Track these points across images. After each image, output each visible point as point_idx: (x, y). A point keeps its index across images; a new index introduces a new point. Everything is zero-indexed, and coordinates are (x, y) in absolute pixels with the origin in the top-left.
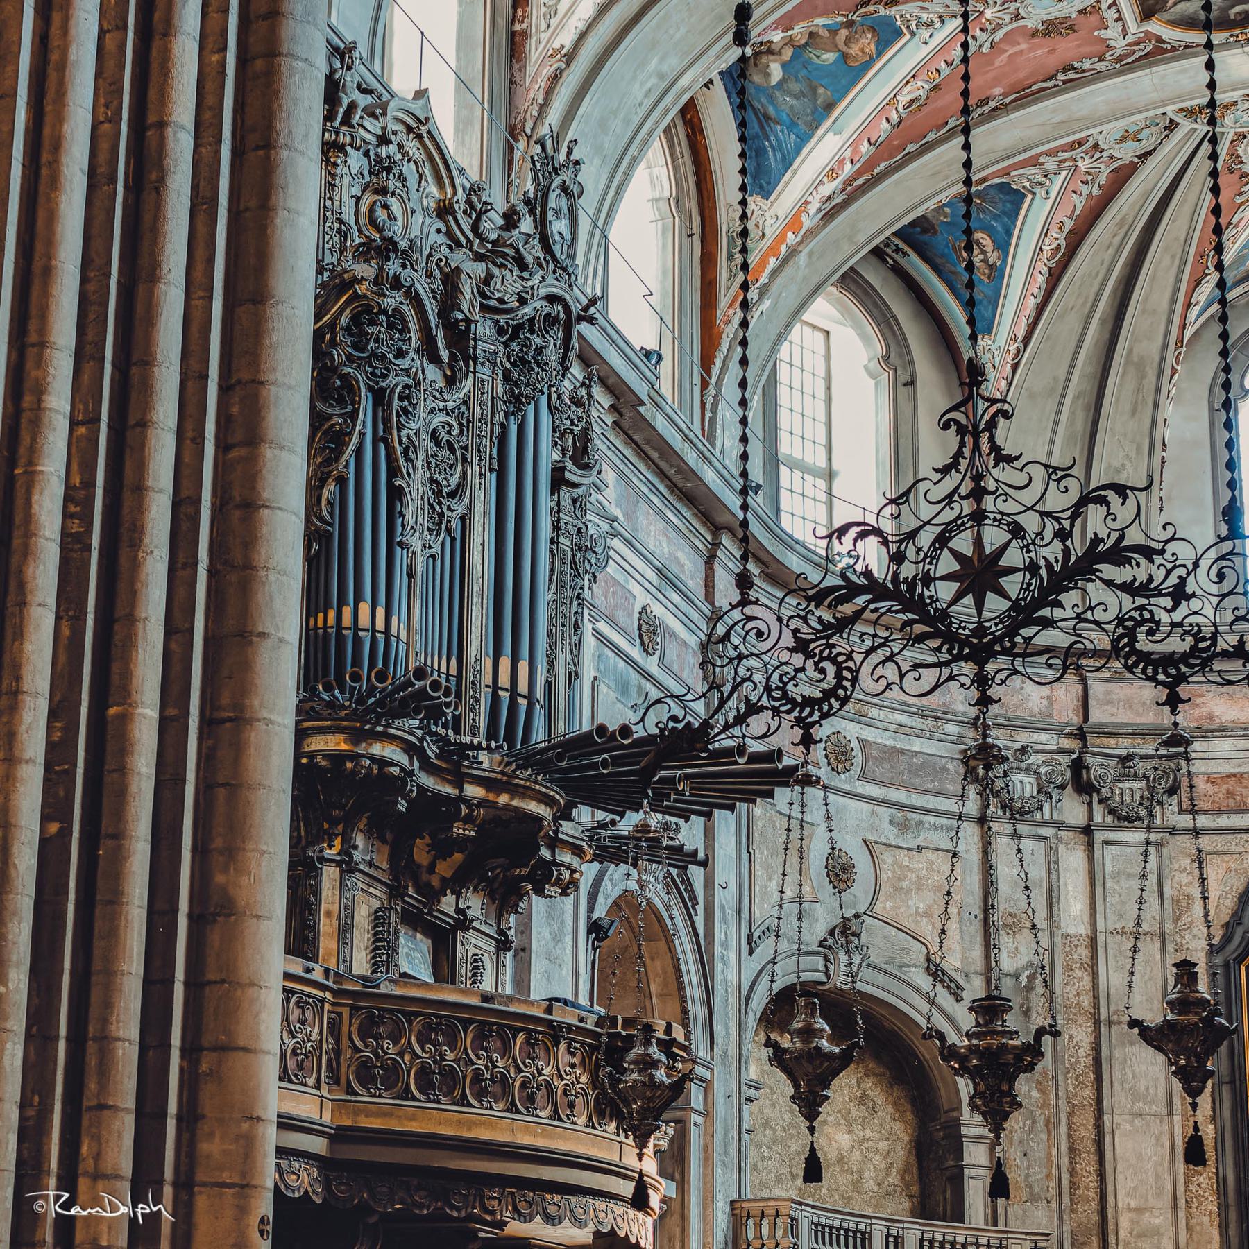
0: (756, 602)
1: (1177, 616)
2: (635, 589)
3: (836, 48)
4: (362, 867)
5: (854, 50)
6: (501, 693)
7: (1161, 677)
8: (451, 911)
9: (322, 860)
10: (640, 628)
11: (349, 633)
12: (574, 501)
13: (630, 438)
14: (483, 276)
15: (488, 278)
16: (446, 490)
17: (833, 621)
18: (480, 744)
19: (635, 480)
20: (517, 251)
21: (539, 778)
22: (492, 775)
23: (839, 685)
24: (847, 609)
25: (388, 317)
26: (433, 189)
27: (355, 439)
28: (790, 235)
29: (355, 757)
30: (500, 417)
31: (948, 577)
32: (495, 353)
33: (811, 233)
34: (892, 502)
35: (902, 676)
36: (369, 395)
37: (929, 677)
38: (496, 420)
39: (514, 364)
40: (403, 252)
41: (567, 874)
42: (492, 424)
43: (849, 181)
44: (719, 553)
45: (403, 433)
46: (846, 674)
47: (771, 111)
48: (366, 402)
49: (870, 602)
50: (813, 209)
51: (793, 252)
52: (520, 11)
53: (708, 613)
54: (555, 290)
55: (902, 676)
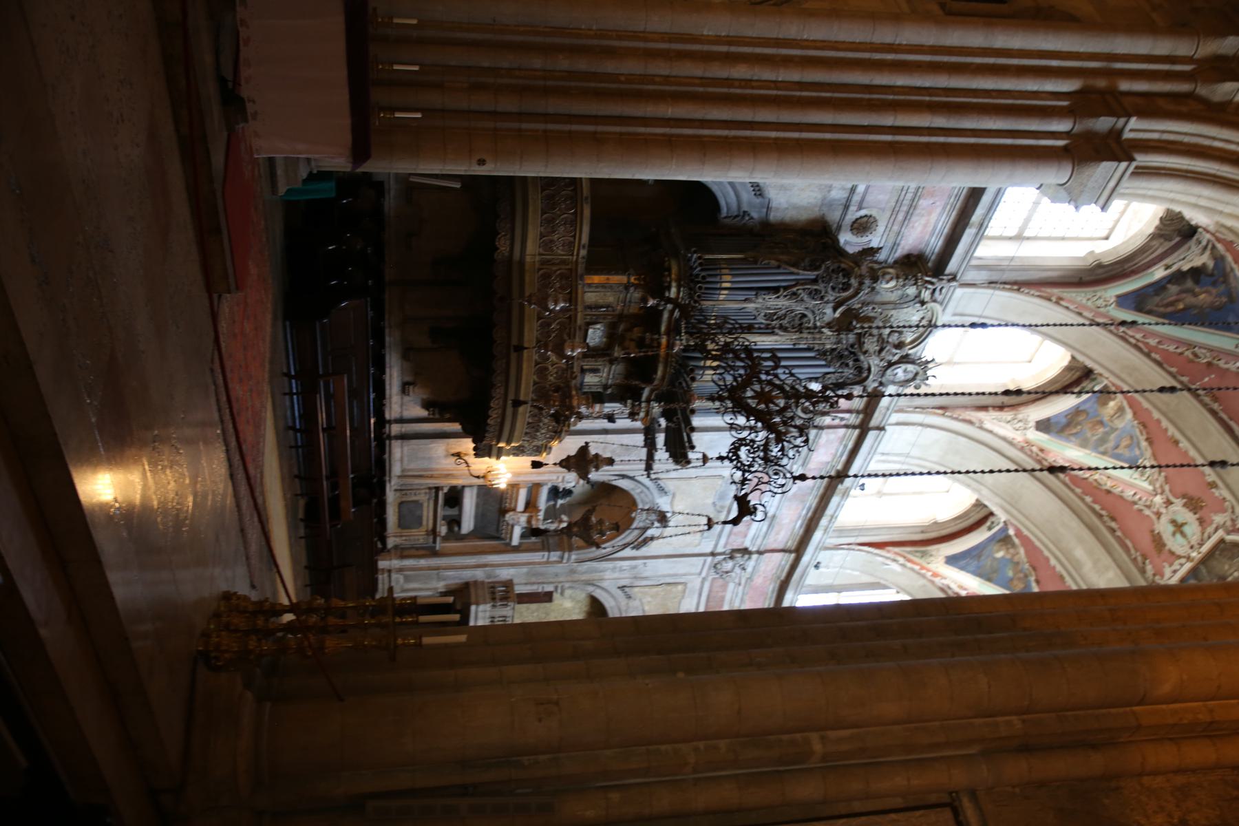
1: (757, 459)
3: (1015, 574)
5: (1015, 582)
7: (731, 455)
9: (629, 274)
11: (718, 272)
26: (909, 340)
27: (793, 270)
28: (930, 574)
29: (670, 275)
30: (817, 347)
31: (762, 388)
32: (842, 344)
33: (932, 582)
36: (814, 277)
37: (721, 383)
39: (839, 353)
47: (983, 558)
48: (812, 275)
50: (945, 582)
51: (924, 576)
52: (997, 409)
54: (873, 369)
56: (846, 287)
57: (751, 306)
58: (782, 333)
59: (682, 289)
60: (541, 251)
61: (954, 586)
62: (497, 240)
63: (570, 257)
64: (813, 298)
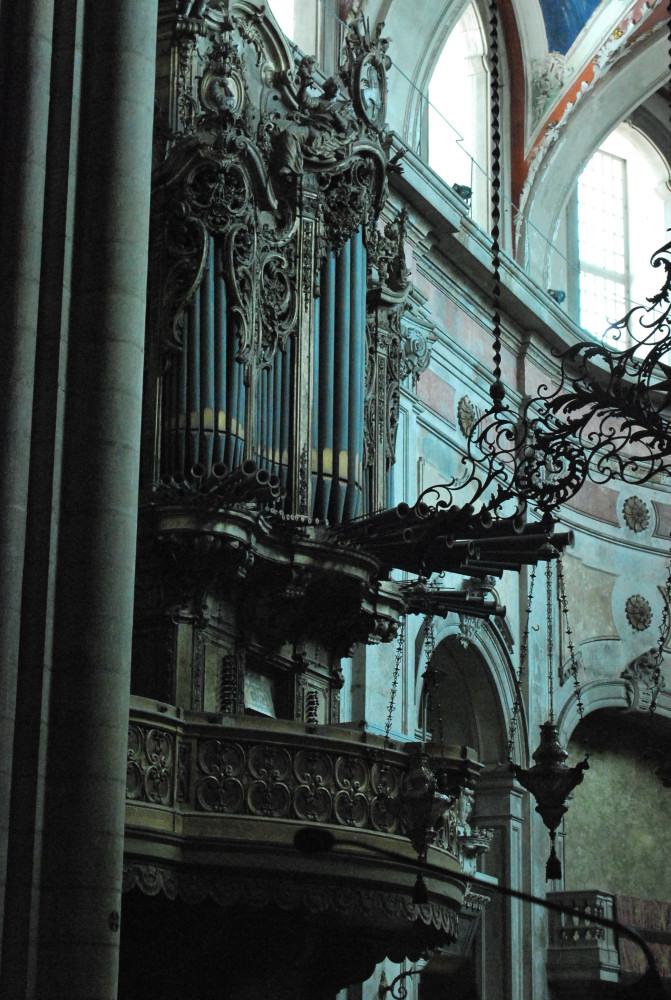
0: (506, 409)
2: (455, 383)
4: (211, 623)
6: (325, 478)
8: (289, 657)
10: (459, 416)
11: (196, 434)
12: (390, 317)
13: (447, 257)
14: (306, 137)
15: (310, 140)
16: (277, 314)
17: (567, 424)
18: (306, 521)
19: (453, 293)
20: (334, 116)
21: (358, 547)
22: (318, 546)
23: (572, 475)
24: (577, 415)
25: (226, 175)
26: (271, 65)
27: (200, 275)
28: (584, 84)
30: (322, 252)
32: (317, 200)
33: (600, 81)
34: (615, 326)
35: (622, 467)
36: (212, 239)
38: (319, 255)
39: (333, 209)
40: (238, 121)
41: (386, 625)
42: (315, 258)
43: (632, 39)
44: (528, 351)
45: (240, 269)
46: (578, 466)
48: (208, 245)
49: (594, 409)
50: (603, 61)
51: (587, 96)
53: (519, 400)
54: (367, 147)
55: (622, 467)
56: (233, 178)
57: (255, 373)
58: (295, 317)
59: (232, 513)
60: (165, 800)
61: (614, 46)
62: (149, 894)
63: (178, 738)
64: (249, 246)
